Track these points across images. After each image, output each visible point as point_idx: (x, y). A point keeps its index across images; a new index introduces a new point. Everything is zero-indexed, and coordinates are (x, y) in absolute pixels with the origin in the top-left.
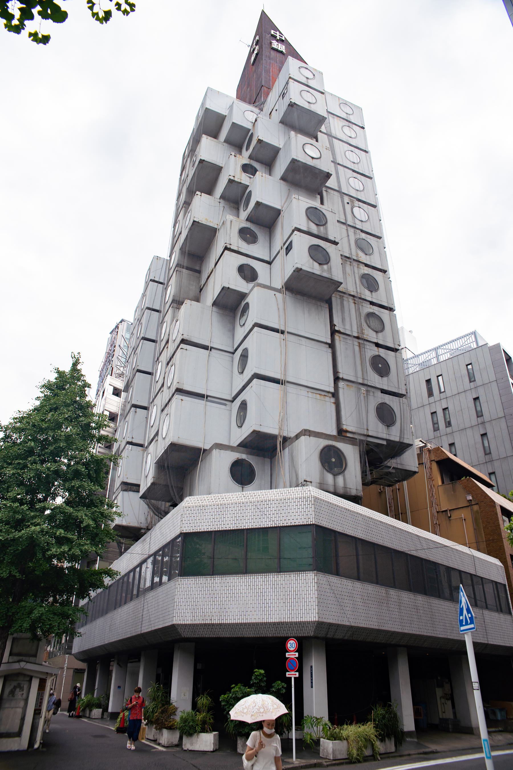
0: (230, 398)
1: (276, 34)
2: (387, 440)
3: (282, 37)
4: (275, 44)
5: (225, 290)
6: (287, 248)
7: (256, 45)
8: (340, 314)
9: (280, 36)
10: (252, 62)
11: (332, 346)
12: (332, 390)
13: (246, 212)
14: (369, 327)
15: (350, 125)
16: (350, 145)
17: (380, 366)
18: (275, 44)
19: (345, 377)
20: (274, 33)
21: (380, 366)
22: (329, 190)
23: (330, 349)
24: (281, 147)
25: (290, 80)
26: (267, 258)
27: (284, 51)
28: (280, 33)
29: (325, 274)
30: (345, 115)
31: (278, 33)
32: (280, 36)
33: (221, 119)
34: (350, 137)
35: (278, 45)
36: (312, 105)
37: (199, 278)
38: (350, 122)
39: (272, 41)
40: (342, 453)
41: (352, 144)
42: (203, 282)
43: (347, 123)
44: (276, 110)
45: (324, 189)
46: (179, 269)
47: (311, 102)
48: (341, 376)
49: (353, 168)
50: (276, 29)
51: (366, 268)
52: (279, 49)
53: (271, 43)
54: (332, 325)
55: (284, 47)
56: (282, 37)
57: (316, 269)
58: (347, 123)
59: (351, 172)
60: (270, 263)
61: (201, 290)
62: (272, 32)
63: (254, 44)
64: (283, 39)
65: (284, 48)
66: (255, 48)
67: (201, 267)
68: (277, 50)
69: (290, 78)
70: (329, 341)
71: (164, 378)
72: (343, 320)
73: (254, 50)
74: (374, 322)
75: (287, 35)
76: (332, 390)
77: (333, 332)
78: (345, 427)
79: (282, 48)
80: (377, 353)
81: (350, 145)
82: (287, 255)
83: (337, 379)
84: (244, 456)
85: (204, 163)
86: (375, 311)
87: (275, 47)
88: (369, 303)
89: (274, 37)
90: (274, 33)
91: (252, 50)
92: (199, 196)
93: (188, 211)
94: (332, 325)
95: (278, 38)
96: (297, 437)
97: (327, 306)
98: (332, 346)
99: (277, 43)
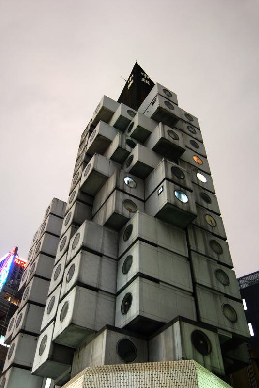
0: (114, 293)
2: (233, 334)
4: (143, 80)
7: (131, 80)
8: (193, 240)
11: (189, 259)
13: (128, 168)
14: (213, 249)
15: (193, 127)
29: (185, 209)
37: (91, 210)
38: (191, 125)
40: (206, 336)
42: (94, 212)
45: (179, 160)
46: (78, 202)
48: (197, 281)
50: (144, 73)
53: (141, 79)
54: (189, 246)
60: (144, 201)
61: (93, 217)
62: (142, 73)
67: (93, 203)
68: (144, 83)
70: (188, 256)
72: (196, 244)
73: (130, 83)
74: (216, 248)
75: (150, 76)
76: (192, 290)
77: (190, 250)
80: (219, 268)
83: (194, 283)
84: (128, 337)
85: (101, 137)
89: (143, 77)
92: (97, 155)
94: (189, 246)
96: (172, 322)
98: (189, 259)
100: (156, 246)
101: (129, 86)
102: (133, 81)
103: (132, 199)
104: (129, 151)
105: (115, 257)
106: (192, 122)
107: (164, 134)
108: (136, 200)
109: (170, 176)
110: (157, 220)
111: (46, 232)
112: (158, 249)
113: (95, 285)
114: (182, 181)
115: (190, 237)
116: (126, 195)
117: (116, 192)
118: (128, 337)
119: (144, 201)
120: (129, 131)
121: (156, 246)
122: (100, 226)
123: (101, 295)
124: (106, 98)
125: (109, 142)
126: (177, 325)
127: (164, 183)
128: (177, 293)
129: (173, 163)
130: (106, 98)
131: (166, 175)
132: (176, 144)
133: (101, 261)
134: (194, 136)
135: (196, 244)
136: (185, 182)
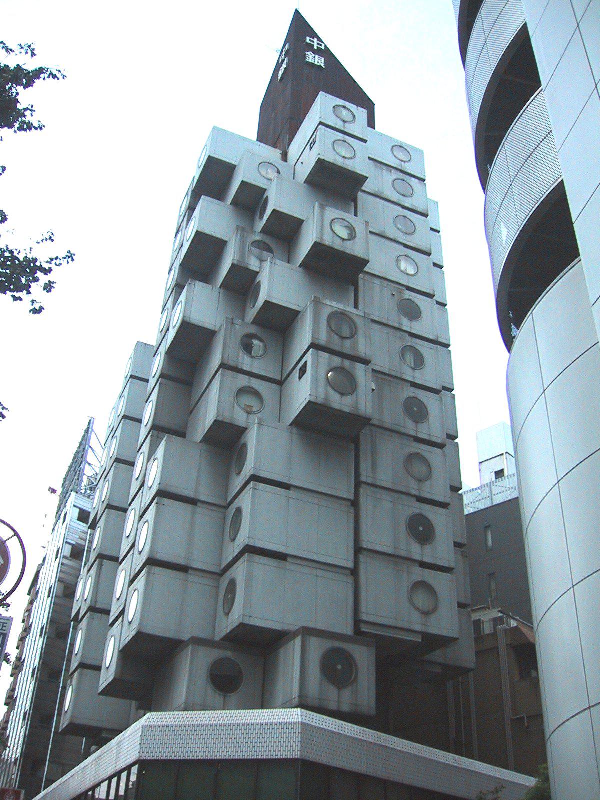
1: (313, 42)
3: (321, 45)
4: (311, 57)
5: (218, 424)
6: (300, 370)
9: (318, 44)
10: (279, 78)
12: (351, 565)
15: (407, 178)
16: (404, 207)
17: (421, 529)
18: (311, 57)
19: (370, 547)
20: (310, 40)
21: (421, 529)
22: (367, 277)
23: (353, 508)
24: (305, 219)
25: (321, 127)
26: (278, 378)
27: (323, 65)
28: (319, 40)
29: (347, 410)
30: (398, 162)
31: (316, 40)
32: (318, 44)
33: (230, 169)
34: (404, 196)
35: (315, 57)
36: (347, 161)
37: (189, 394)
39: (307, 53)
41: (406, 205)
42: (193, 402)
43: (401, 176)
44: (302, 163)
46: (165, 381)
47: (347, 156)
49: (405, 242)
50: (314, 35)
51: (412, 389)
52: (316, 63)
55: (323, 59)
56: (321, 45)
57: (338, 402)
58: (402, 175)
59: (402, 248)
61: (191, 413)
63: (284, 53)
64: (323, 47)
65: (323, 62)
66: (284, 59)
69: (321, 124)
71: (136, 535)
73: (283, 61)
76: (351, 565)
77: (358, 484)
78: (364, 617)
79: (320, 62)
80: (417, 511)
81: (404, 207)
82: (300, 379)
83: (358, 550)
86: (419, 451)
87: (311, 61)
88: (412, 439)
89: (310, 47)
90: (310, 40)
91: (281, 60)
93: (178, 302)
95: (316, 48)
97: (353, 446)
98: (355, 504)
99: (314, 56)
100: (287, 487)
101: (281, 73)
102: (289, 61)
103: (256, 384)
104: (257, 270)
105: (223, 503)
106: (407, 165)
107: (322, 235)
108: (263, 383)
109: (323, 339)
110: (295, 430)
111: (125, 417)
112: (292, 493)
113: (182, 562)
114: (348, 343)
115: (362, 455)
116: (241, 376)
117: (223, 375)
118: (229, 654)
119: (281, 383)
120: (261, 218)
121: (287, 487)
122: (196, 443)
123: (192, 577)
124: (218, 133)
125: (220, 245)
126: (298, 641)
127: (309, 358)
128: (320, 573)
129: (334, 304)
130: (218, 133)
131: (313, 337)
132: (348, 252)
133: (194, 513)
134: (407, 203)
135: (374, 466)
136: (355, 346)
